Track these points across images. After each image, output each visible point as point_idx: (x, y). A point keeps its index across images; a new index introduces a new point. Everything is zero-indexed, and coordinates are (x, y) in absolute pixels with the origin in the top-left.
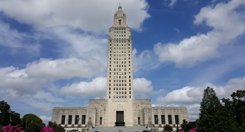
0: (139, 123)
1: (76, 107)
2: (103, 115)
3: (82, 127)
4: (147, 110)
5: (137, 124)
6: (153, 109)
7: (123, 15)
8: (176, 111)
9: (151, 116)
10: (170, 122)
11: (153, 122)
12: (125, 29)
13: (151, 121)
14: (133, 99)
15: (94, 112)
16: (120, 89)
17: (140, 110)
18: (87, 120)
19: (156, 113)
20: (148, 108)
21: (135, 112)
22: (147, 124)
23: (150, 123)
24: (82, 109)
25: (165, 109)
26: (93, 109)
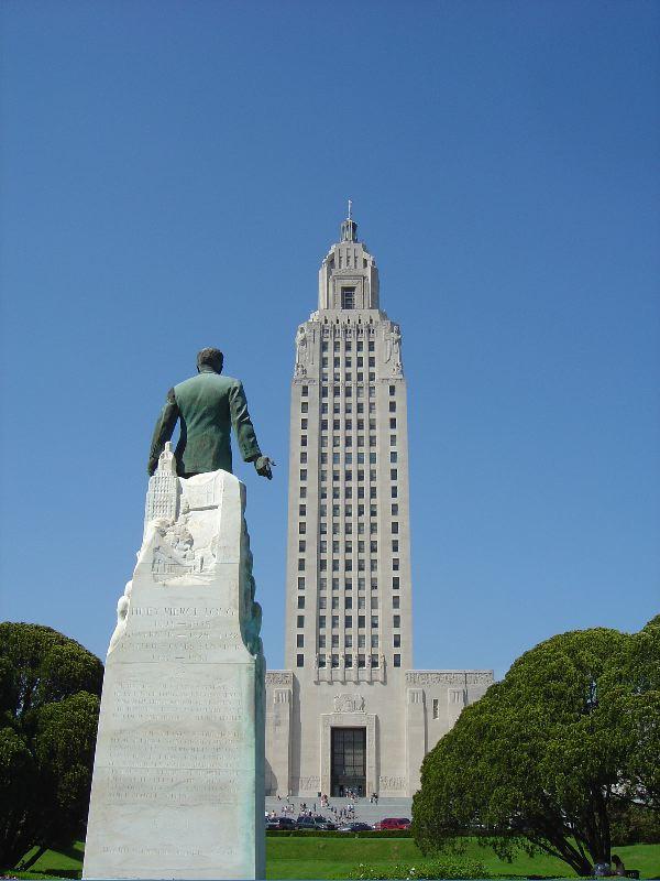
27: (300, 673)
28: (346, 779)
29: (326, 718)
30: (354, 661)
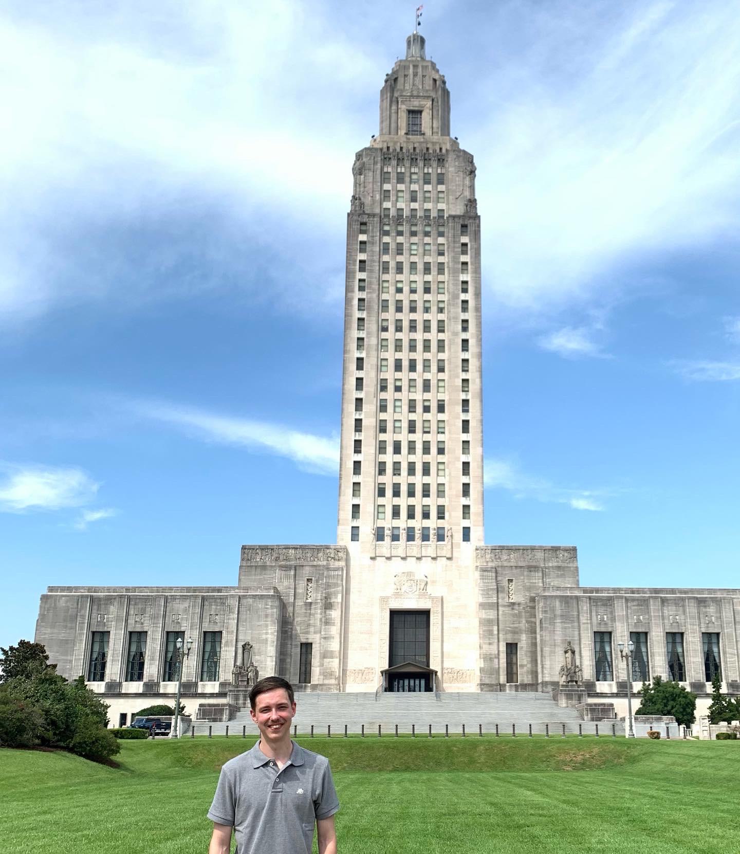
0: (511, 675)
1: (171, 589)
2: (315, 633)
3: (203, 695)
4: (558, 603)
5: (503, 679)
6: (590, 598)
7: (431, 82)
8: (712, 610)
9: (577, 638)
10: (677, 667)
11: (588, 671)
12: (441, 160)
13: (578, 663)
14: (482, 544)
15: (267, 616)
16: (411, 494)
17: (516, 607)
18: (228, 657)
19: (602, 619)
20: (562, 598)
21: (492, 615)
22: (556, 679)
23: (572, 673)
24: (204, 599)
25: (651, 601)
26: (262, 597)
27: (353, 547)
28: (408, 671)
29: (384, 600)
30: (418, 534)
